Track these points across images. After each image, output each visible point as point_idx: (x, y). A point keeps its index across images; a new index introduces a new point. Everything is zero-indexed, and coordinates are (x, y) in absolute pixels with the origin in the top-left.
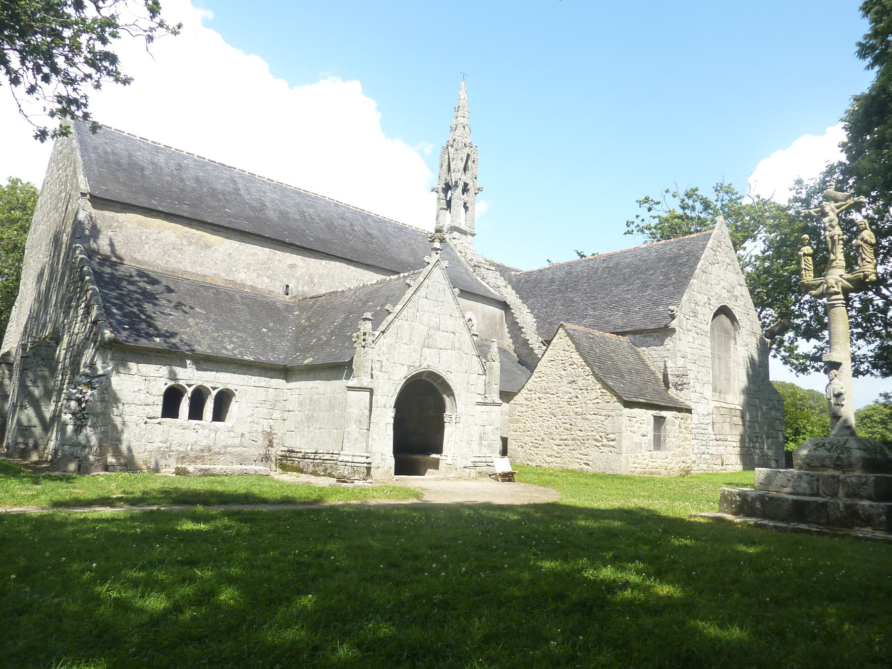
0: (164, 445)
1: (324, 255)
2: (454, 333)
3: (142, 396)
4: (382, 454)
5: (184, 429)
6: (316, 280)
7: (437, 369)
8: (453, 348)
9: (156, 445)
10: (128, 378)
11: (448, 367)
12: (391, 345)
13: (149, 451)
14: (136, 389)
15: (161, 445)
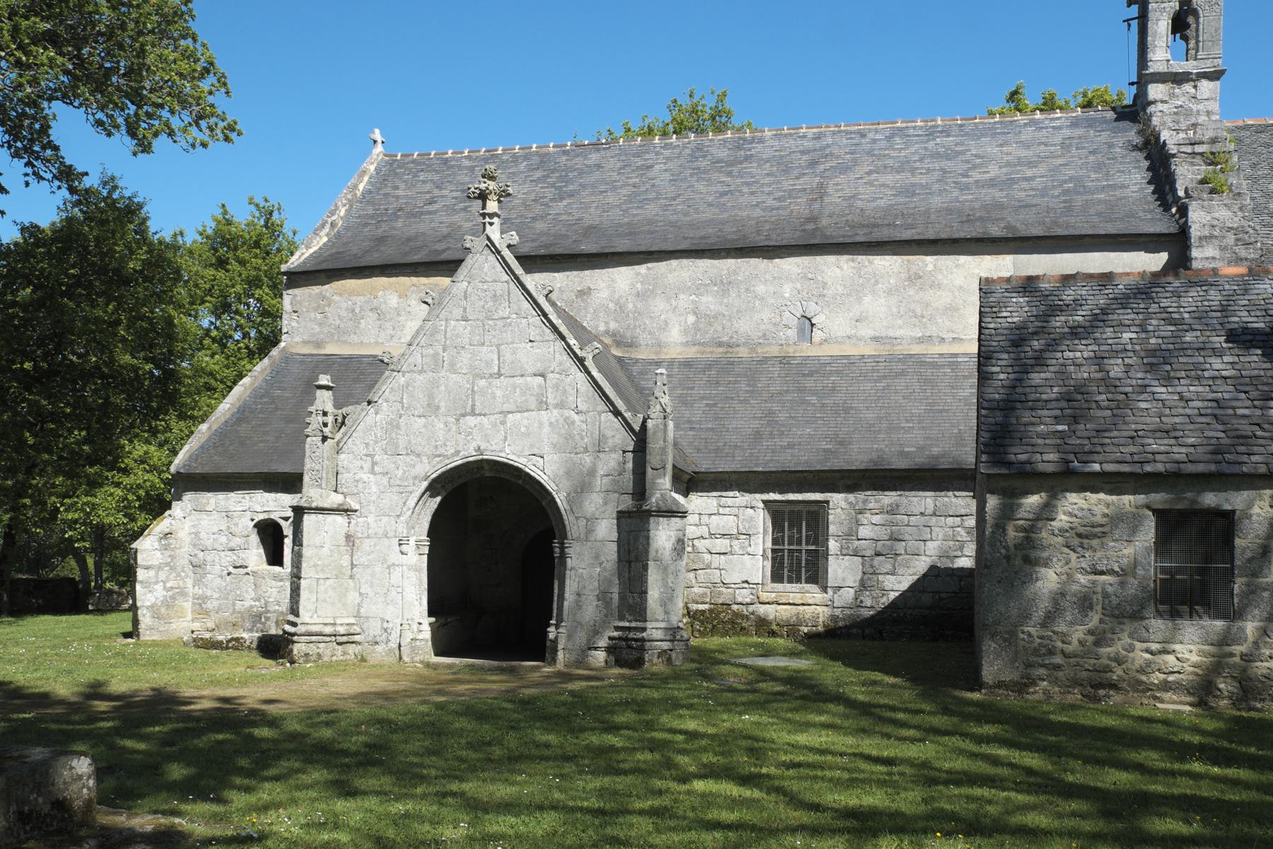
0: (257, 603)
1: (642, 256)
2: (543, 375)
3: (223, 539)
4: (383, 620)
5: (281, 580)
6: (630, 306)
7: (501, 454)
8: (543, 405)
9: (247, 604)
10: (205, 516)
11: (532, 446)
12: (391, 423)
13: (239, 612)
14: (215, 529)
15: (253, 603)
